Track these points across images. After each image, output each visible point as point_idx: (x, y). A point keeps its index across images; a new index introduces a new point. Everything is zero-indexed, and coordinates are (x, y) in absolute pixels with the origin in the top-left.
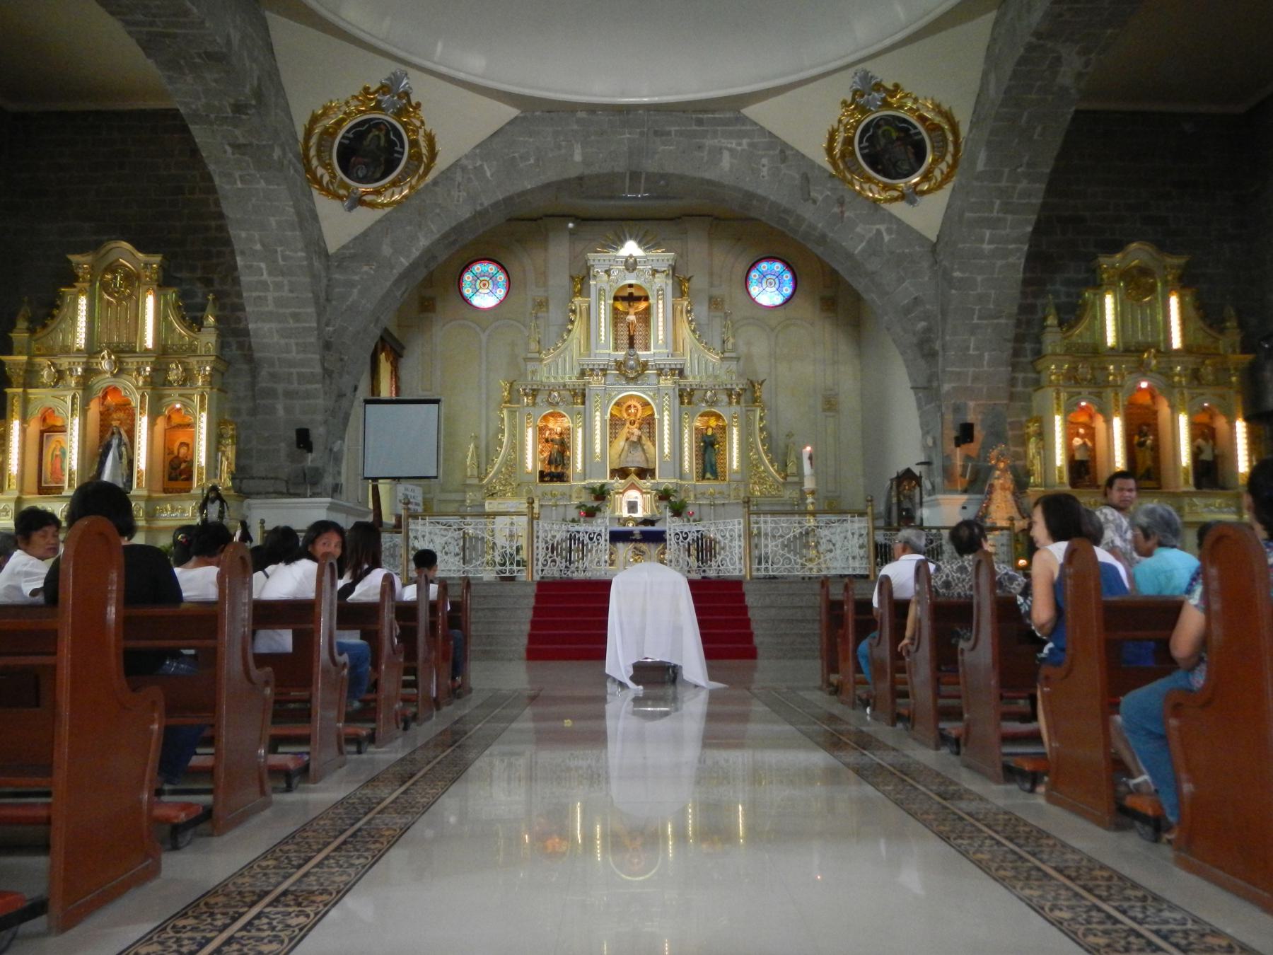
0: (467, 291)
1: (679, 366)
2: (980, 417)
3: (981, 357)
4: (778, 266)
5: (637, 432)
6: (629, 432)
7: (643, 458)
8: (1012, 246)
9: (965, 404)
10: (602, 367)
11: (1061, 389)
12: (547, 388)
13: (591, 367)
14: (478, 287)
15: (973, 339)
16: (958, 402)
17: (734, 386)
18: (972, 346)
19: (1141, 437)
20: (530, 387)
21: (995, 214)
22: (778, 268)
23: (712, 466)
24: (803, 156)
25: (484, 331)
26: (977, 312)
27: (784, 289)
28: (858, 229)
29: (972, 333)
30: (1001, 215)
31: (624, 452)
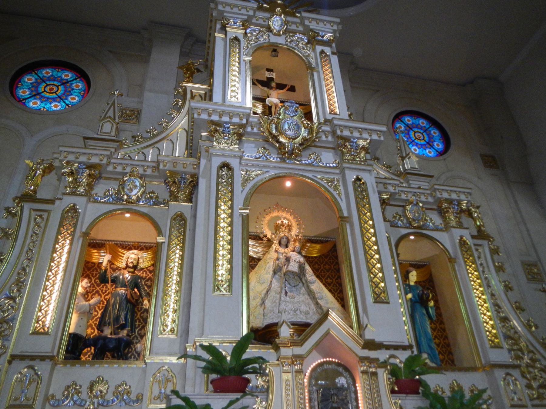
0: (23, 92)
1: (375, 137)
4: (422, 122)
5: (295, 257)
6: (278, 259)
7: (313, 306)
10: (236, 120)
12: (119, 169)
13: (215, 118)
14: (41, 88)
17: (454, 196)
20: (83, 159)
22: (423, 123)
25: (32, 136)
27: (435, 144)
31: (272, 294)
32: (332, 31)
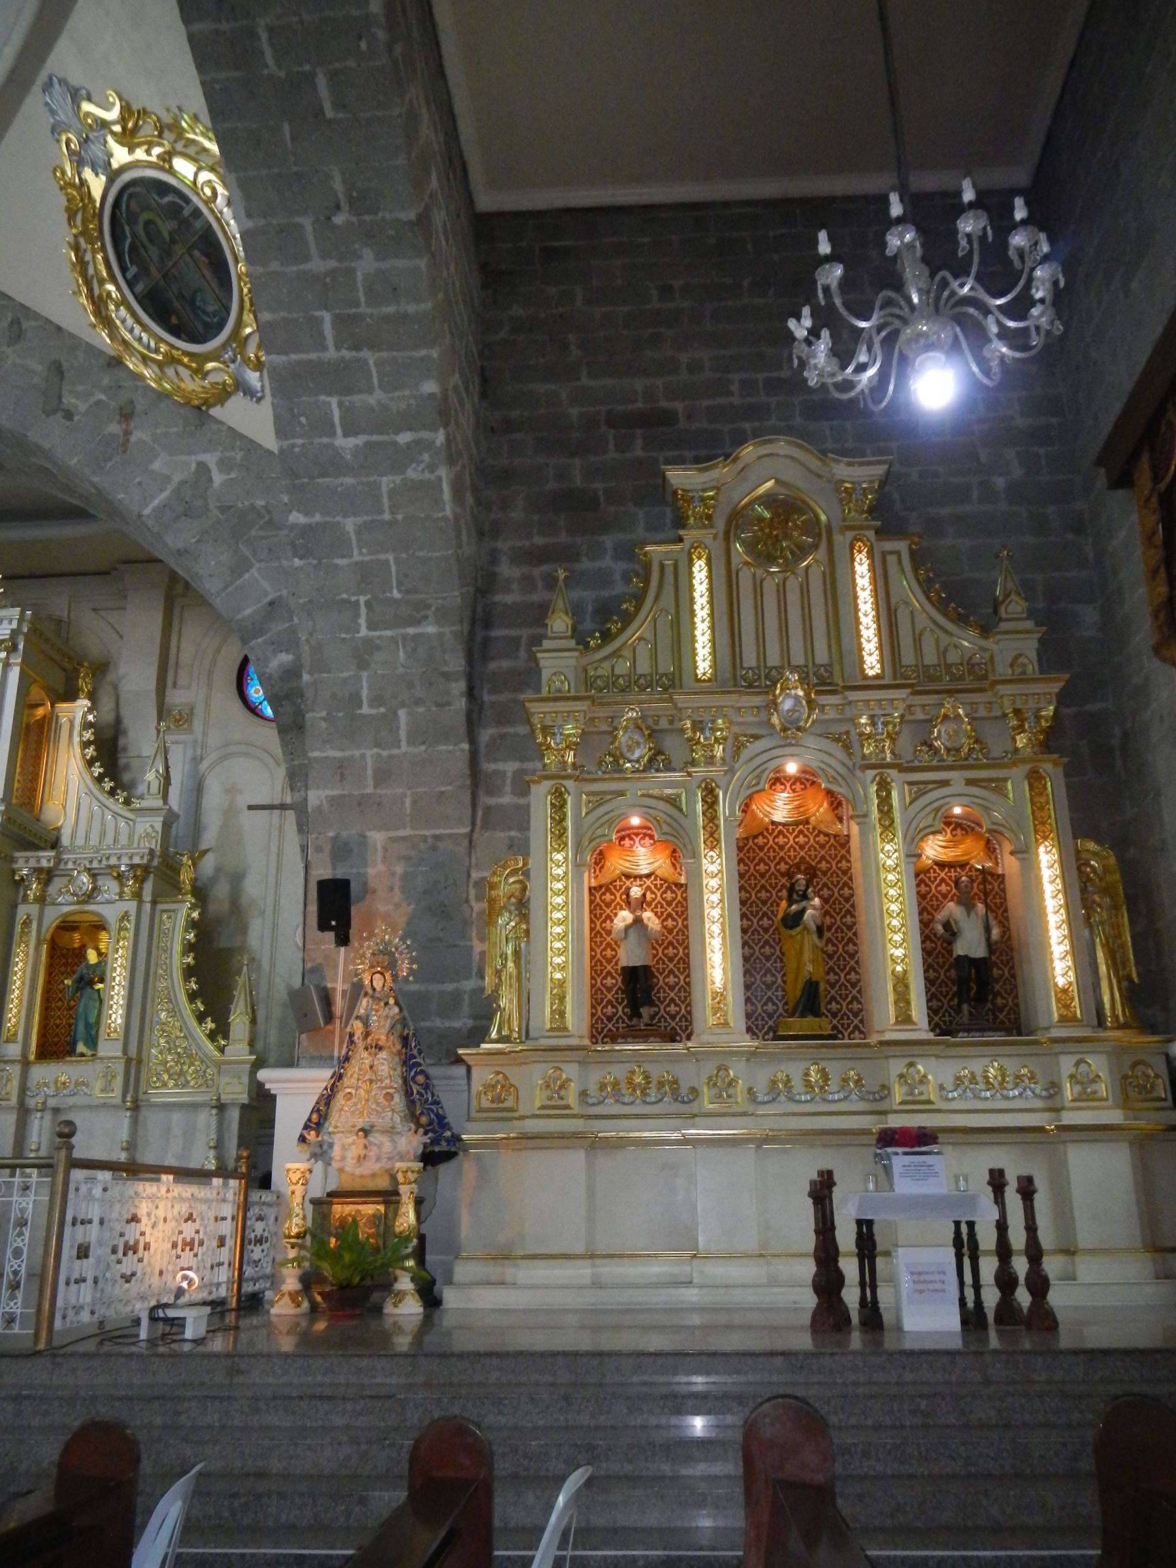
2: (399, 869)
3: (390, 720)
8: (405, 438)
9: (365, 837)
11: (570, 784)
15: (365, 674)
16: (344, 834)
18: (364, 693)
19: (791, 902)
21: (332, 353)
23: (88, 1026)
24: (59, 328)
26: (363, 611)
28: (156, 465)
29: (362, 665)
30: (346, 354)
32: (9, 632)
